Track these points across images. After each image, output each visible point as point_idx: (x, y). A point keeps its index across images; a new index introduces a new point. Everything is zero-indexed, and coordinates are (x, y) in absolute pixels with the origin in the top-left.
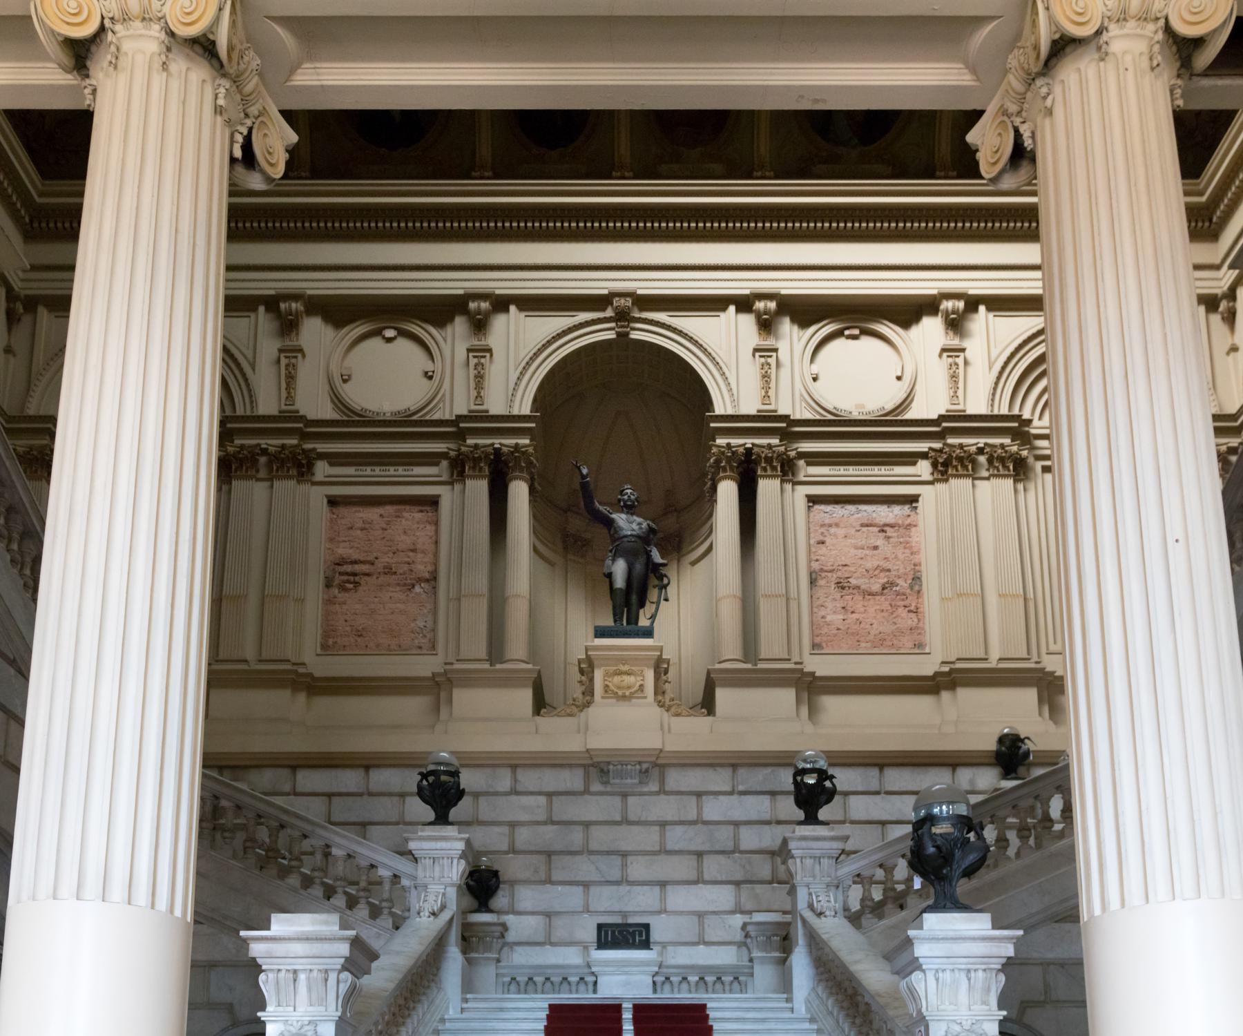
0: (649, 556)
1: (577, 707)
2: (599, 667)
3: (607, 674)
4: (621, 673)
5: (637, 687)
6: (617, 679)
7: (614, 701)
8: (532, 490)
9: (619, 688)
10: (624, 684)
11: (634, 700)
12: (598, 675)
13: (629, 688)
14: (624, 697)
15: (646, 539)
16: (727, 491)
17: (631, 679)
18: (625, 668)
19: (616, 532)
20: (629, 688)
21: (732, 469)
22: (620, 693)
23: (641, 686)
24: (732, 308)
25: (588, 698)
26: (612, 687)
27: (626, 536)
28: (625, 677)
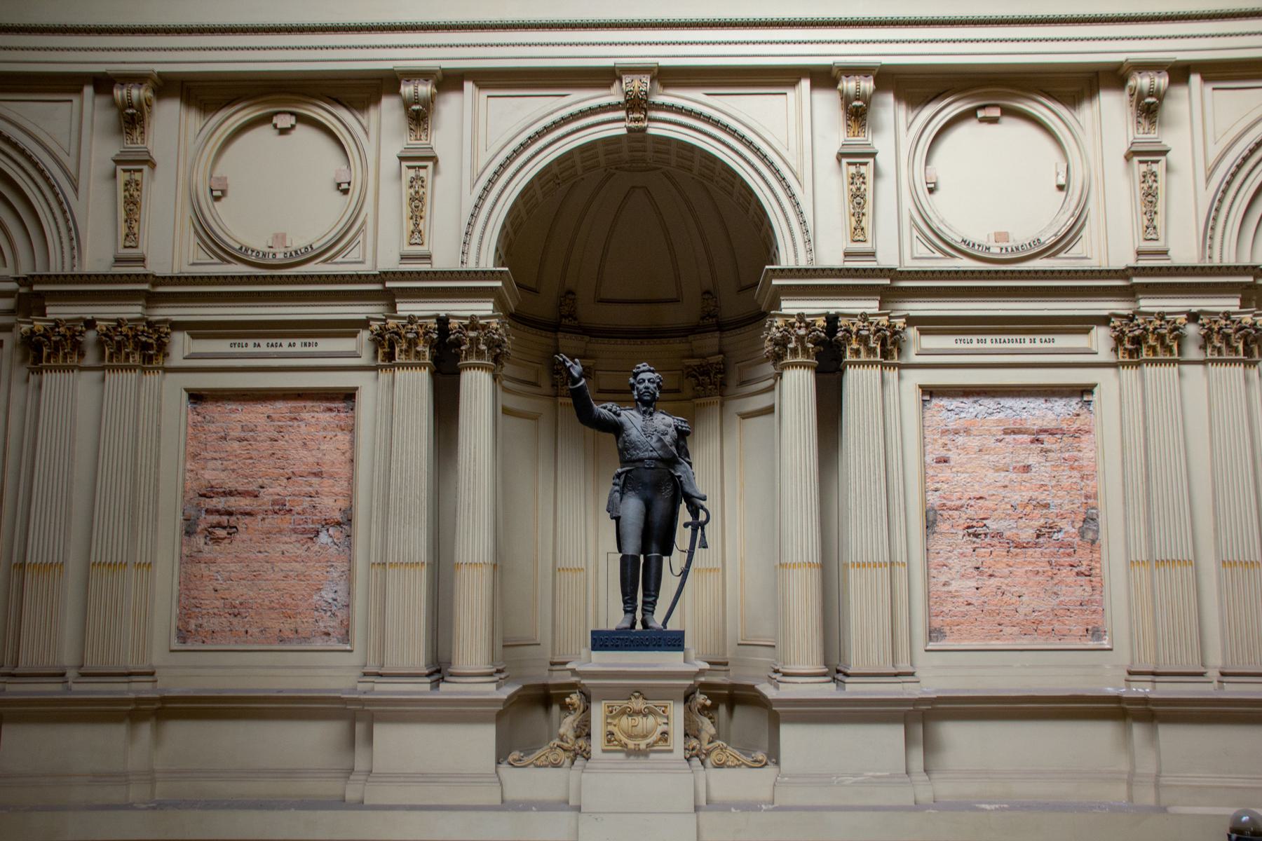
4: (634, 713)
6: (625, 722)
7: (621, 756)
10: (639, 730)
11: (652, 756)
16: (798, 384)
20: (645, 737)
23: (664, 733)
24: (805, 84)
28: (639, 720)
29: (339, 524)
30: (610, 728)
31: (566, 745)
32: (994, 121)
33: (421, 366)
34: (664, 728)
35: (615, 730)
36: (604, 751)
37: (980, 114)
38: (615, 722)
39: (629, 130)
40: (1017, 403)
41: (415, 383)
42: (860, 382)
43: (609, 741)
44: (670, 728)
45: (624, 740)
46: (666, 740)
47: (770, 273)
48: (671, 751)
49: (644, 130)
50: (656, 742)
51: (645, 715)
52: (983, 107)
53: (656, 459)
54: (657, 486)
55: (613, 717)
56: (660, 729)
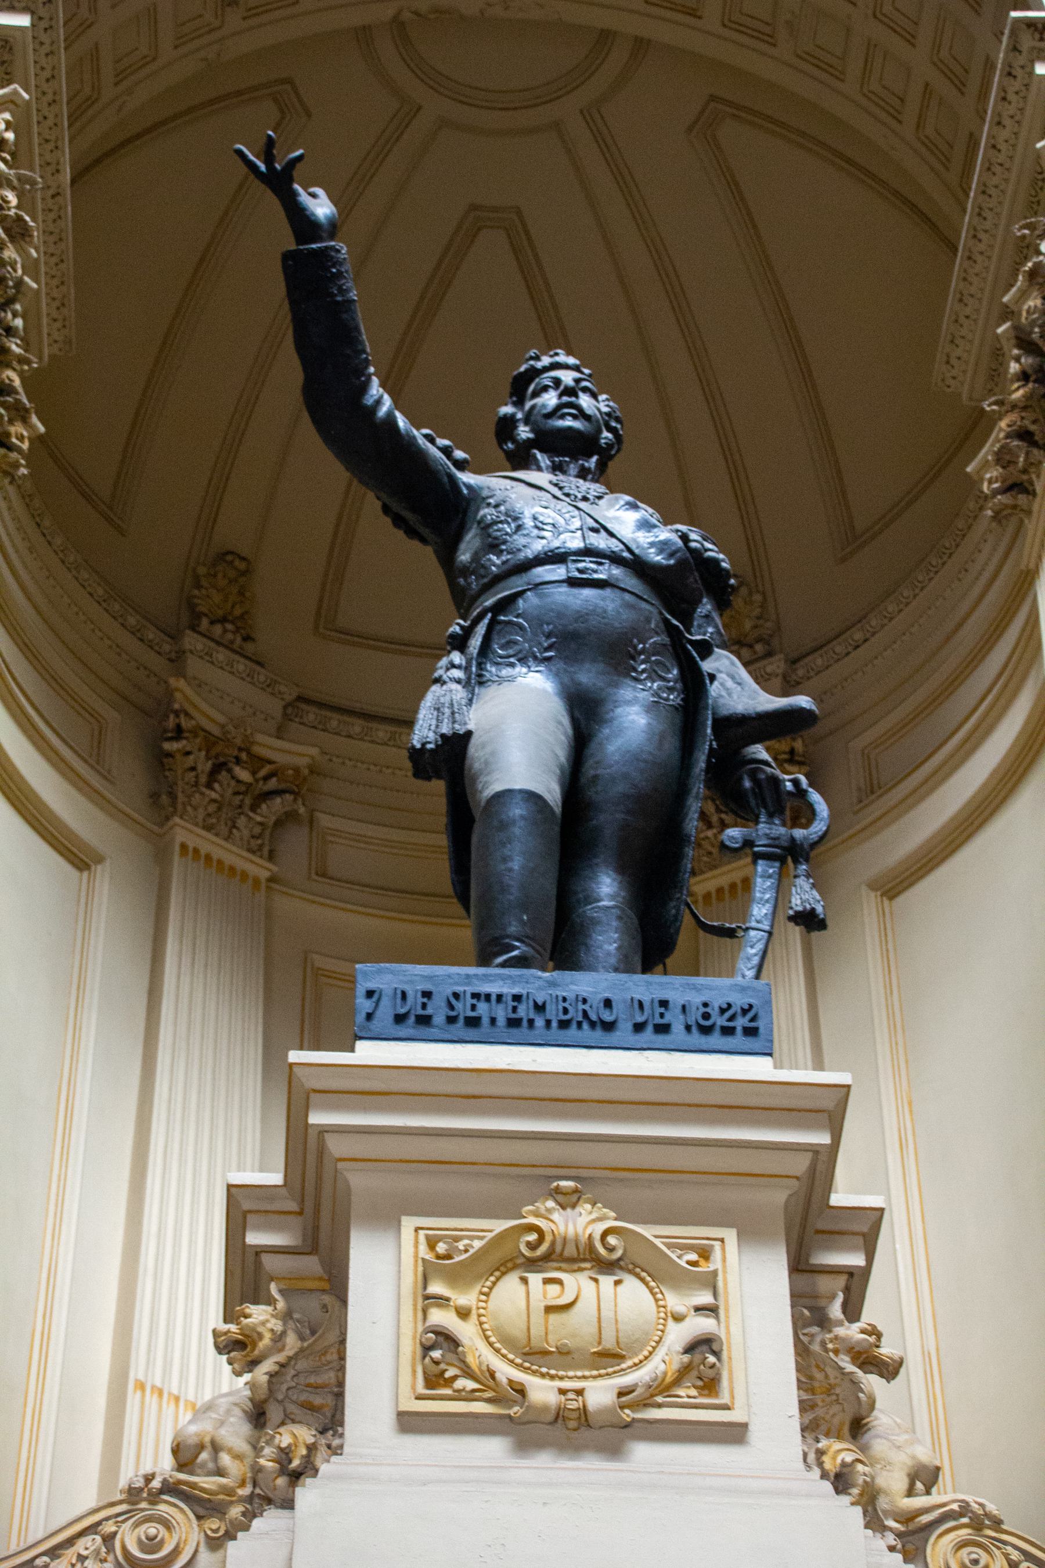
0: (694, 685)
1: (205, 1506)
2: (387, 1216)
3: (442, 1266)
5: (664, 1361)
6: (515, 1298)
7: (492, 1448)
9: (535, 1355)
10: (577, 1328)
11: (644, 1454)
12: (381, 1273)
13: (608, 1358)
14: (573, 1430)
15: (677, 585)
17: (629, 1300)
18: (581, 1222)
19: (494, 546)
20: (608, 1358)
25: (295, 1436)
26: (479, 1351)
27: (557, 557)
28: (577, 1284)
30: (439, 1317)
34: (705, 1325)
35: (466, 1332)
36: (409, 1423)
38: (467, 1298)
43: (435, 1380)
45: (505, 1372)
46: (710, 1385)
47: (1027, 41)
48: (734, 1434)
50: (662, 1389)
51: (607, 1266)
53: (615, 559)
54: (618, 653)
55: (461, 1274)
56: (678, 1336)
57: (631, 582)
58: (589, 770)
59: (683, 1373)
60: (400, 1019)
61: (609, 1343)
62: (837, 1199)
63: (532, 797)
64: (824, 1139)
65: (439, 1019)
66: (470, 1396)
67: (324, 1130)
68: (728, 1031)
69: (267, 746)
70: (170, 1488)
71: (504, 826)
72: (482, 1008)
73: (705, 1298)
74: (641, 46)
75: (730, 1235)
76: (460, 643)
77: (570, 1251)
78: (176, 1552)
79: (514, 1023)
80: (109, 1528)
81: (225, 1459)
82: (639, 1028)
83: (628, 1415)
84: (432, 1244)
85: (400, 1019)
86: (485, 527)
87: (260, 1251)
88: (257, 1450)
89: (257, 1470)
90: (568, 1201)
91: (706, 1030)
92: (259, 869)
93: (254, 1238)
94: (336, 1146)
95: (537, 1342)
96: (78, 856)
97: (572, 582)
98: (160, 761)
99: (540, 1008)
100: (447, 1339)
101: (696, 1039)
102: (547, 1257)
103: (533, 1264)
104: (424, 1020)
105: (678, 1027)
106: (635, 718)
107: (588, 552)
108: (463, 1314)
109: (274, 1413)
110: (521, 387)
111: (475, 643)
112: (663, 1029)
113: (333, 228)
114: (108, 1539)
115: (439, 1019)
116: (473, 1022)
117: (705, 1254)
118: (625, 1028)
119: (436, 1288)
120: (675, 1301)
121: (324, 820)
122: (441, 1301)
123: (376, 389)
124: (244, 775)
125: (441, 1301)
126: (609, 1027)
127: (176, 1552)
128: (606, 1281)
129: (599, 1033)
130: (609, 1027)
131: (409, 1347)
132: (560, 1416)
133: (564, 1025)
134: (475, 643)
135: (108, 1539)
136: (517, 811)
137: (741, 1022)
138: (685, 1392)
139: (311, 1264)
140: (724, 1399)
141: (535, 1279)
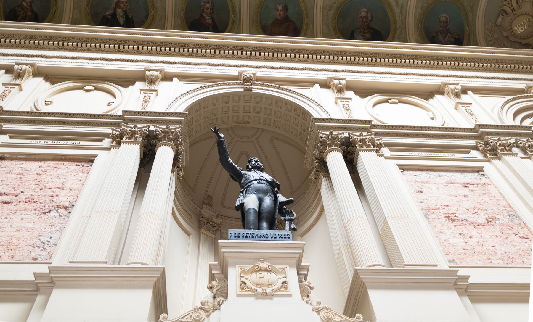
0: (276, 198)
1: (206, 311)
2: (234, 265)
3: (242, 272)
4: (259, 270)
5: (279, 284)
6: (255, 276)
7: (252, 299)
8: (176, 158)
9: (258, 285)
10: (265, 281)
11: (276, 299)
12: (233, 274)
13: (270, 285)
14: (264, 295)
18: (265, 265)
19: (247, 179)
20: (270, 285)
21: (336, 146)
22: (260, 290)
23: (284, 282)
24: (317, 86)
25: (220, 299)
26: (249, 284)
28: (264, 274)
29: (66, 208)
31: (206, 307)
32: (396, 103)
33: (136, 143)
34: (284, 280)
36: (238, 295)
37: (390, 101)
38: (247, 277)
39: (246, 90)
40: (449, 174)
41: (132, 152)
42: (366, 159)
43: (242, 289)
44: (288, 280)
45: (254, 287)
46: (286, 289)
47: (314, 120)
48: (290, 296)
49: (250, 90)
50: (279, 289)
51: (269, 271)
52: (391, 99)
53: (264, 180)
54: (265, 192)
55: (246, 273)
57: (267, 183)
58: (262, 208)
59: (282, 286)
60: (235, 237)
61: (270, 283)
62: (302, 264)
63: (254, 209)
64: (301, 252)
65: (241, 237)
66: (248, 291)
67: (224, 252)
68: (285, 238)
69: (215, 220)
70: (201, 308)
71: (250, 213)
72: (248, 235)
73: (285, 276)
74: (263, 130)
75: (288, 267)
76: (242, 192)
77: (263, 269)
78: (202, 318)
79: (253, 237)
80: (191, 314)
81: (209, 304)
82: (272, 238)
83: (273, 293)
84: (241, 269)
85: (235, 237)
86: (245, 177)
87: (214, 274)
88: (214, 302)
89: (214, 305)
90: (262, 262)
91: (282, 238)
92: (213, 236)
93: (213, 272)
94: (226, 255)
95: (258, 283)
96: (188, 234)
97: (258, 183)
98: (200, 222)
99: (257, 235)
100: (245, 283)
101: (280, 239)
102: (259, 270)
103: (257, 271)
104: (239, 237)
105: (278, 237)
106: (268, 201)
107: (260, 179)
108: (247, 279)
109: (217, 296)
110: (250, 162)
111: (244, 192)
112: (275, 238)
113: (224, 138)
114: (191, 316)
115: (241, 237)
116: (246, 237)
117: (284, 269)
118: (270, 238)
119: (242, 275)
120: (280, 276)
121: (222, 230)
122: (243, 277)
123: (229, 159)
124: (211, 223)
125: (243, 277)
126: (267, 237)
127: (202, 318)
128: (269, 273)
129: (266, 239)
130: (267, 237)
131: (238, 284)
132: (262, 294)
133: (260, 237)
134: (244, 192)
135: (191, 316)
136: (252, 211)
137: (287, 237)
138: (282, 289)
139: (222, 276)
140: (288, 290)
141: (258, 273)
